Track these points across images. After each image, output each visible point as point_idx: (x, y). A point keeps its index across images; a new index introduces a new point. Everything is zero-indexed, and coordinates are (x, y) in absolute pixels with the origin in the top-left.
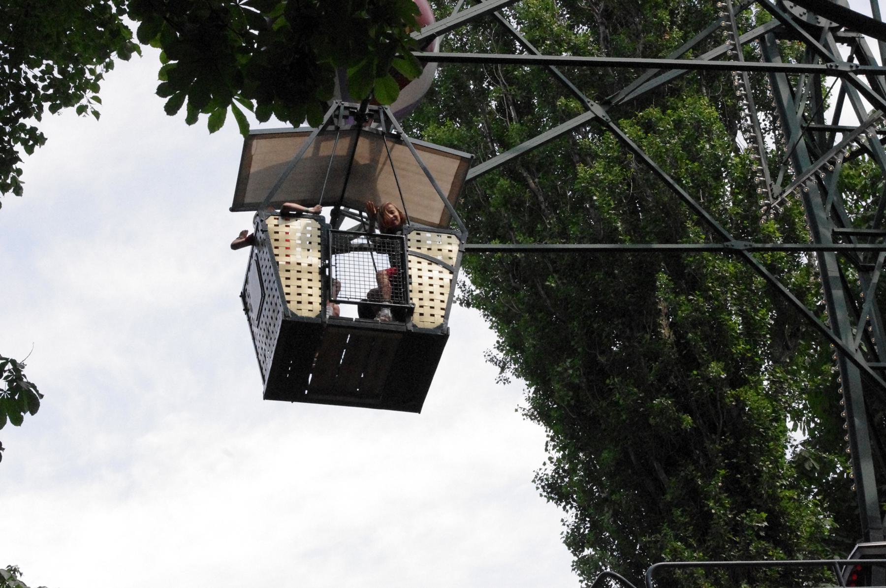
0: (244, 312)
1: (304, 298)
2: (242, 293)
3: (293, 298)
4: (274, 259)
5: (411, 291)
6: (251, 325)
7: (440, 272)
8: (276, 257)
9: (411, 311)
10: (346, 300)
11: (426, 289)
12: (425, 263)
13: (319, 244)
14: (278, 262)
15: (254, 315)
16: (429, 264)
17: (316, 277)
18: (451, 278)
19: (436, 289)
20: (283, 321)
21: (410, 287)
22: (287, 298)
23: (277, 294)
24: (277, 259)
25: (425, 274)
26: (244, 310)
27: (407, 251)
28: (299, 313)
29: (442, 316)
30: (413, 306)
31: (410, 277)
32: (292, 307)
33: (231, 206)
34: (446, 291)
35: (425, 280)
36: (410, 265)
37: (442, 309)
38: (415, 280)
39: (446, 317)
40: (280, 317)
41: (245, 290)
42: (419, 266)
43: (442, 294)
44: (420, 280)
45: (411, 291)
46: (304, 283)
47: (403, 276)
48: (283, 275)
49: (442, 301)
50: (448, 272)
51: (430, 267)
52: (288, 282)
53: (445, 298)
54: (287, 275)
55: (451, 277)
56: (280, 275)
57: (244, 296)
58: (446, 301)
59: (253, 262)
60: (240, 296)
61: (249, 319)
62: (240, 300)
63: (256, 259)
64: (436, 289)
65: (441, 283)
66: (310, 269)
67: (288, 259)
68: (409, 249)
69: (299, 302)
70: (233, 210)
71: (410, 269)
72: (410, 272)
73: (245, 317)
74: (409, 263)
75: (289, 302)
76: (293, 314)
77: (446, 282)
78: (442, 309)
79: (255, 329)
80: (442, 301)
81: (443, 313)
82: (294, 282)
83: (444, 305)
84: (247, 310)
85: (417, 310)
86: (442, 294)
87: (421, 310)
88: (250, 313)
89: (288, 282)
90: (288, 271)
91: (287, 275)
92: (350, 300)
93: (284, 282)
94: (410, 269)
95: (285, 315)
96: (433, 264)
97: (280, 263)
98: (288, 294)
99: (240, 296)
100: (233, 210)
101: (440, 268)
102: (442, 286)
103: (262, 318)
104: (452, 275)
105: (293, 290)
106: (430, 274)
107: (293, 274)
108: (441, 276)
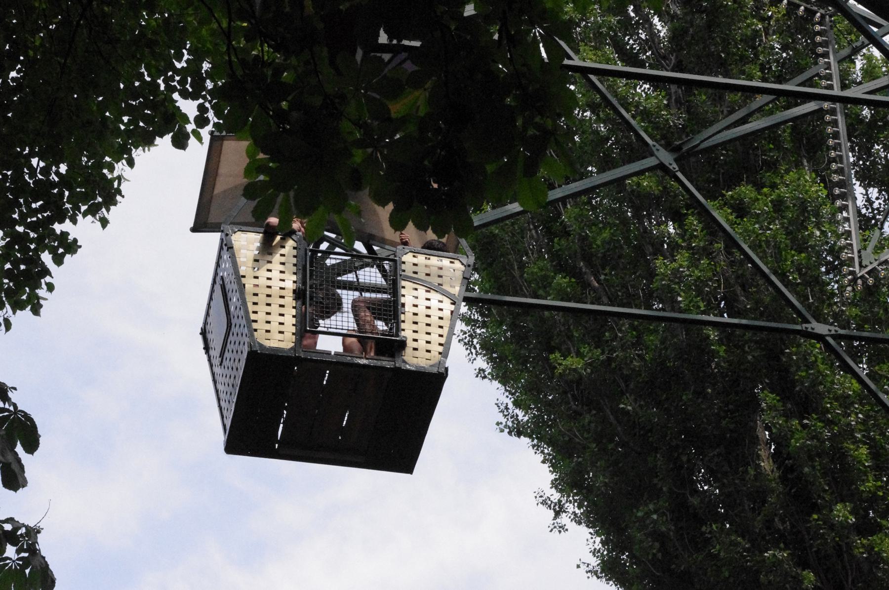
0: (203, 351)
1: (274, 327)
2: (202, 329)
3: (260, 326)
4: (241, 280)
5: (403, 321)
6: (211, 366)
7: (441, 301)
8: (243, 279)
9: (402, 344)
10: (325, 330)
11: (421, 319)
12: (422, 291)
13: (295, 265)
14: (244, 285)
15: (215, 353)
16: (427, 291)
17: (289, 301)
18: (453, 309)
19: (434, 320)
20: (249, 353)
21: (402, 317)
22: (255, 326)
23: (244, 322)
24: (244, 280)
25: (422, 303)
26: (204, 348)
27: (401, 275)
28: (267, 344)
29: (440, 353)
30: (404, 339)
31: (403, 305)
32: (260, 337)
33: (192, 226)
34: (446, 323)
35: (421, 310)
36: (403, 291)
37: (440, 344)
38: (408, 308)
39: (444, 354)
40: (246, 349)
41: (205, 323)
42: (415, 293)
43: (441, 327)
44: (415, 310)
45: (403, 321)
46: (274, 308)
47: (394, 303)
48: (250, 299)
49: (441, 336)
50: (450, 301)
51: (428, 295)
52: (255, 308)
53: (445, 331)
54: (255, 299)
55: (453, 307)
56: (247, 300)
57: (204, 333)
58: (445, 335)
59: (218, 288)
60: (201, 334)
61: (209, 360)
62: (200, 338)
63: (221, 283)
64: (434, 320)
65: (440, 314)
66: (283, 293)
67: (256, 281)
68: (403, 273)
69: (268, 331)
70: (194, 229)
71: (404, 296)
72: (403, 300)
73: (205, 357)
74: (403, 290)
75: (256, 330)
76: (261, 345)
77: (446, 314)
78: (440, 344)
79: (217, 370)
80: (441, 336)
81: (441, 349)
82: (262, 309)
83: (443, 340)
84: (207, 348)
85: (410, 344)
86: (441, 327)
87: (415, 345)
88: (212, 352)
89: (255, 308)
90: (256, 295)
91: (255, 299)
92: (330, 330)
93: (251, 308)
94: (404, 296)
95: (250, 346)
96: (431, 291)
97: (246, 286)
98: (256, 321)
99: (201, 334)
100: (194, 229)
101: (440, 297)
102: (441, 318)
103: (227, 355)
104: (453, 306)
105: (261, 317)
106: (428, 303)
107: (262, 299)
108: (441, 306)
